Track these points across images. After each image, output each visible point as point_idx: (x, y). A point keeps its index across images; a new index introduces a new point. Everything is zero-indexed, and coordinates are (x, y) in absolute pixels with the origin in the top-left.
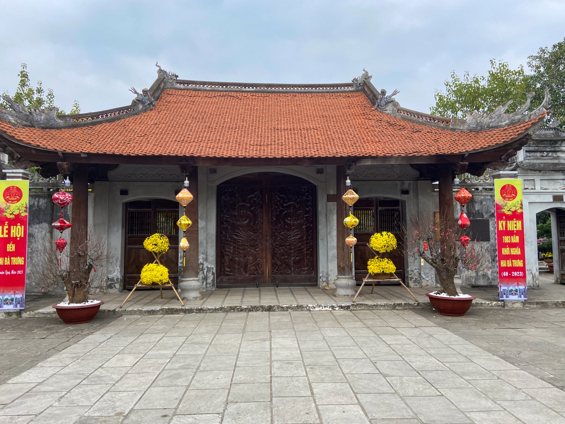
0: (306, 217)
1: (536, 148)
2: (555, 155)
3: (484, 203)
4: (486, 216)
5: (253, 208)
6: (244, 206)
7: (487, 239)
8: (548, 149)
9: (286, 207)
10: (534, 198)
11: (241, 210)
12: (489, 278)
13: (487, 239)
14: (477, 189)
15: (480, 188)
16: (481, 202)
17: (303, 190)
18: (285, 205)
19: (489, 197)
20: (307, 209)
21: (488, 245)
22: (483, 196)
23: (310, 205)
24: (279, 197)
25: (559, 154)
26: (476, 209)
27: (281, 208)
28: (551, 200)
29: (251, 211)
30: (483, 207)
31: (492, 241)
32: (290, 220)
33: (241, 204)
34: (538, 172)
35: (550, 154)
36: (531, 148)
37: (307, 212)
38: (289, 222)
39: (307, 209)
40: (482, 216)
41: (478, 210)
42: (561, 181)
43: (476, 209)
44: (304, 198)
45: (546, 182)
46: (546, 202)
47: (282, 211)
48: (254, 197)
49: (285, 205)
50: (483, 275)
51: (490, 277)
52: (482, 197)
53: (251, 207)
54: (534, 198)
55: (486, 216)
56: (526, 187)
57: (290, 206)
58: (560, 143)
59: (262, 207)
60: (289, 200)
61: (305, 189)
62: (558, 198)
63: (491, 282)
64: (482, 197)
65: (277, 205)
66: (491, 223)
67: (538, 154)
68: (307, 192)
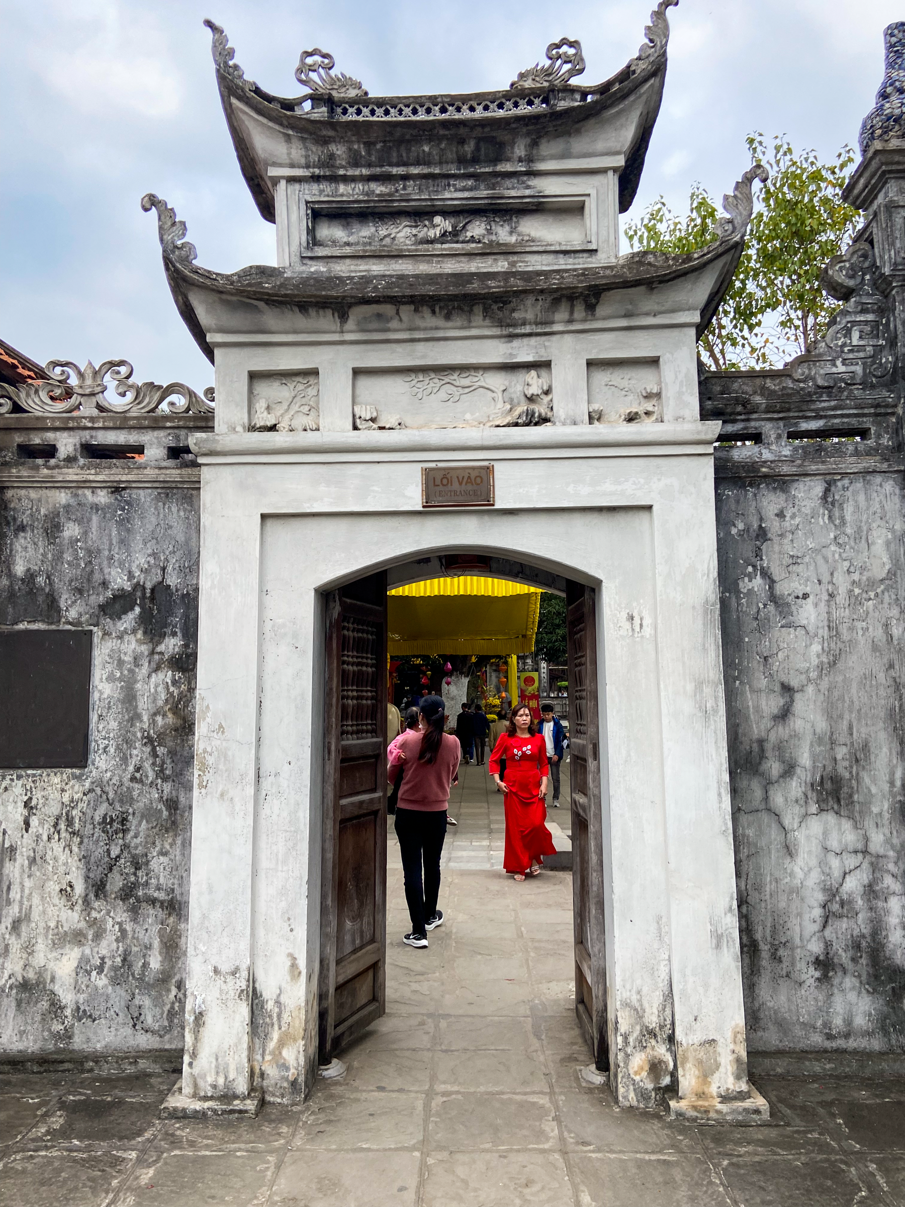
1: (379, 189)
2: (503, 234)
3: (71, 530)
4: (73, 611)
7: (71, 752)
8: (453, 195)
10: (299, 488)
12: (56, 1007)
13: (71, 752)
14: (50, 451)
15: (66, 444)
16: (52, 528)
19: (103, 497)
21: (76, 790)
22: (64, 486)
25: (536, 229)
26: (20, 569)
28: (414, 499)
30: (58, 558)
31: (102, 763)
34: (327, 320)
35: (477, 229)
36: (347, 192)
40: (52, 608)
41: (30, 576)
42: (496, 381)
43: (20, 569)
45: (396, 386)
46: (370, 517)
50: (25, 986)
51: (67, 997)
52: (62, 497)
54: (299, 488)
55: (73, 611)
56: (263, 418)
58: (520, 150)
62: (458, 488)
63: (68, 1035)
64: (62, 497)
66: (101, 652)
67: (402, 234)
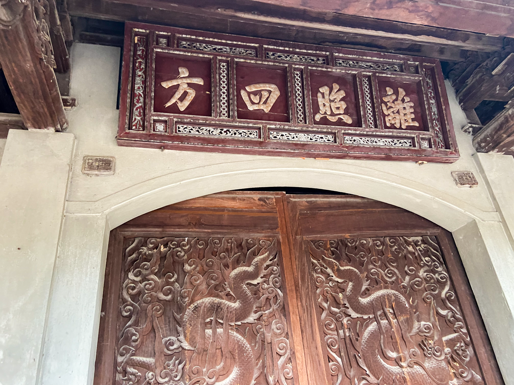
0: (451, 343)
5: (251, 318)
6: (216, 309)
9: (372, 308)
11: (206, 325)
17: (410, 248)
18: (364, 301)
20: (444, 312)
23: (448, 298)
24: (340, 273)
27: (354, 315)
29: (251, 333)
32: (397, 362)
33: (208, 300)
37: (447, 325)
38: (395, 369)
39: (444, 312)
44: (422, 273)
47: (358, 326)
48: (254, 275)
49: (364, 301)
53: (242, 314)
57: (381, 302)
59: (284, 310)
60: (376, 283)
61: (416, 244)
65: (337, 304)
68: (426, 253)
